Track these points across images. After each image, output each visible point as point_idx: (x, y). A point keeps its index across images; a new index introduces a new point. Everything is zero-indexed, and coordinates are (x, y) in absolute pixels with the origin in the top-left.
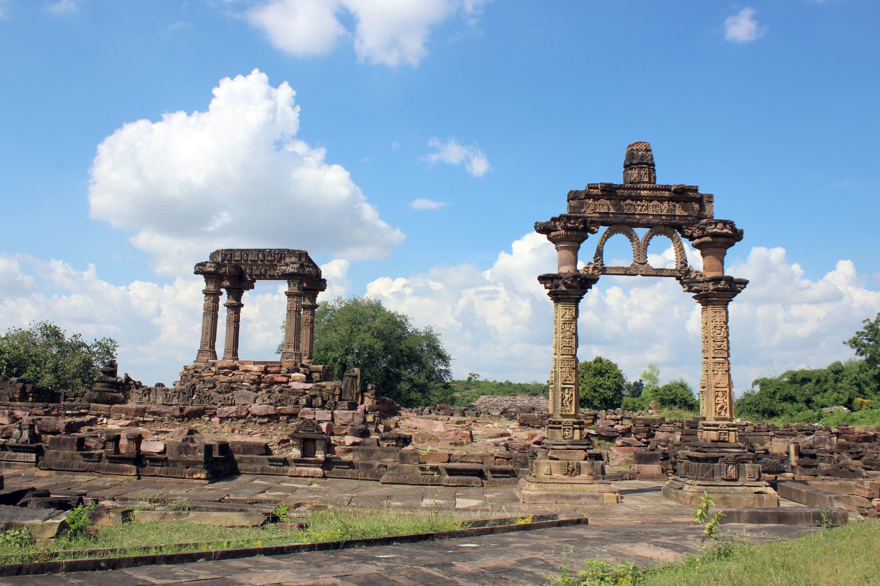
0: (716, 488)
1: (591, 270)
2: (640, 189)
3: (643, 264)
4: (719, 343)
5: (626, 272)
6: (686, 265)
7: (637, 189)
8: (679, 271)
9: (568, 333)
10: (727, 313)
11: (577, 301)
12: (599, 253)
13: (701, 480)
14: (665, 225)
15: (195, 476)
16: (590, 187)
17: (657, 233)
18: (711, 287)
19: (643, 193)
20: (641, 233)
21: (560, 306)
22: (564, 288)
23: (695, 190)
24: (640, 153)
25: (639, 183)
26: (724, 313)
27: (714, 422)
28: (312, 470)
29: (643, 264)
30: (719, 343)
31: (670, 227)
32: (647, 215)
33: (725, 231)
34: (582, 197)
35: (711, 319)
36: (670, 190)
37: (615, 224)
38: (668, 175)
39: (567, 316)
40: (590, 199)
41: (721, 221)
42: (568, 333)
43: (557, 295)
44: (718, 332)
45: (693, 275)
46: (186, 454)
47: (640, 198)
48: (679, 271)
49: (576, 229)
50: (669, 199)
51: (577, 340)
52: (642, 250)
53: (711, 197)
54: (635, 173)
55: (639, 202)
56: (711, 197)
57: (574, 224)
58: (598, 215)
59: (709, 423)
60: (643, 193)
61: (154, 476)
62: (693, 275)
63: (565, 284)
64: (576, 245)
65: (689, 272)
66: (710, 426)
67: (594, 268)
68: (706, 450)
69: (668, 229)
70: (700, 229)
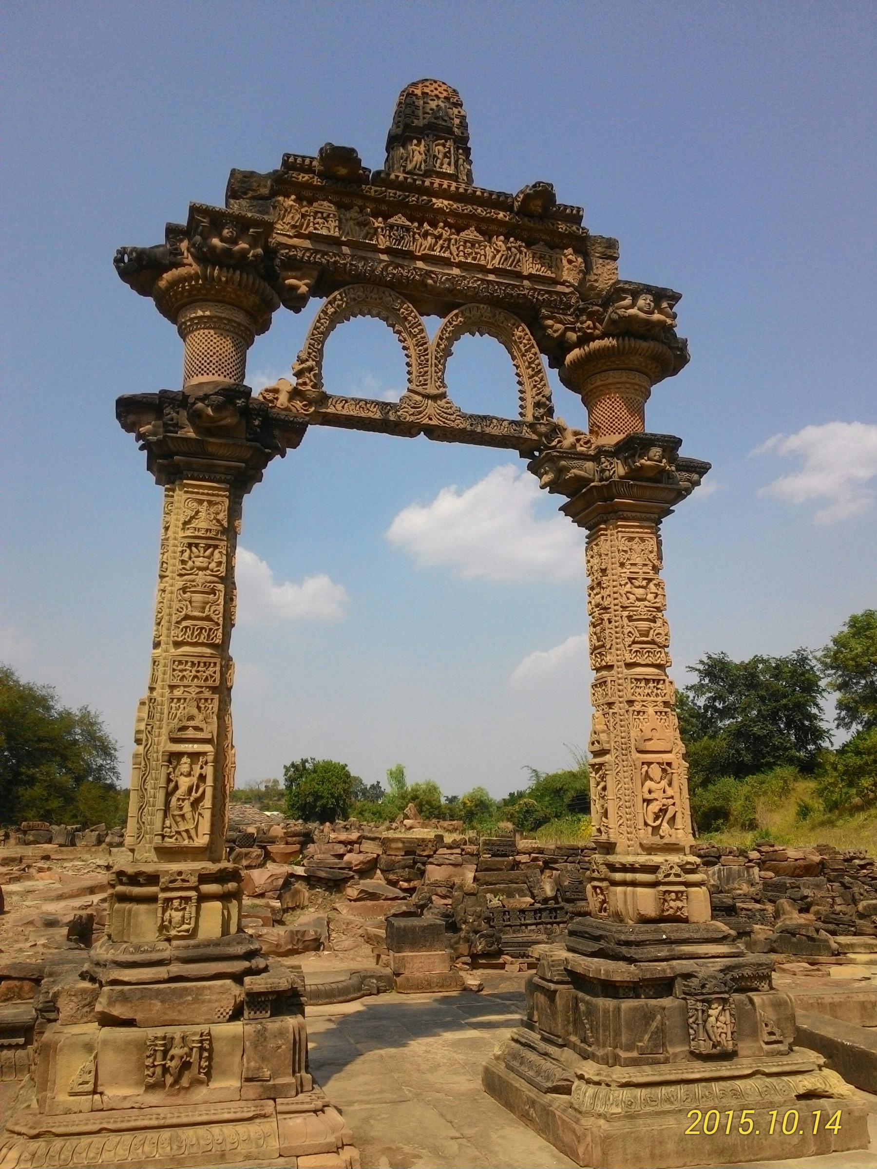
1: (283, 399)
3: (435, 398)
4: (644, 625)
5: (387, 422)
6: (550, 412)
8: (531, 426)
9: (201, 577)
10: (659, 543)
11: (241, 480)
13: (634, 1063)
14: (495, 302)
16: (291, 164)
17: (474, 326)
18: (621, 470)
19: (439, 203)
21: (180, 495)
22: (190, 433)
23: (575, 216)
24: (433, 104)
25: (429, 173)
26: (652, 544)
27: (643, 859)
29: (435, 398)
30: (644, 625)
31: (507, 311)
32: (447, 263)
33: (656, 316)
34: (265, 191)
35: (619, 557)
36: (509, 208)
37: (360, 279)
39: (202, 524)
40: (287, 196)
41: (648, 289)
42: (201, 577)
43: (170, 455)
44: (640, 592)
45: (570, 440)
47: (433, 217)
48: (531, 426)
49: (239, 262)
50: (509, 231)
51: (229, 599)
52: (430, 363)
53: (611, 244)
54: (417, 153)
55: (426, 226)
56: (611, 244)
57: (234, 241)
58: (307, 244)
59: (629, 859)
60: (439, 203)
62: (570, 440)
63: (196, 417)
64: (240, 318)
65: (557, 430)
66: (632, 869)
67: (295, 393)
68: (632, 952)
69: (501, 315)
70: (591, 316)
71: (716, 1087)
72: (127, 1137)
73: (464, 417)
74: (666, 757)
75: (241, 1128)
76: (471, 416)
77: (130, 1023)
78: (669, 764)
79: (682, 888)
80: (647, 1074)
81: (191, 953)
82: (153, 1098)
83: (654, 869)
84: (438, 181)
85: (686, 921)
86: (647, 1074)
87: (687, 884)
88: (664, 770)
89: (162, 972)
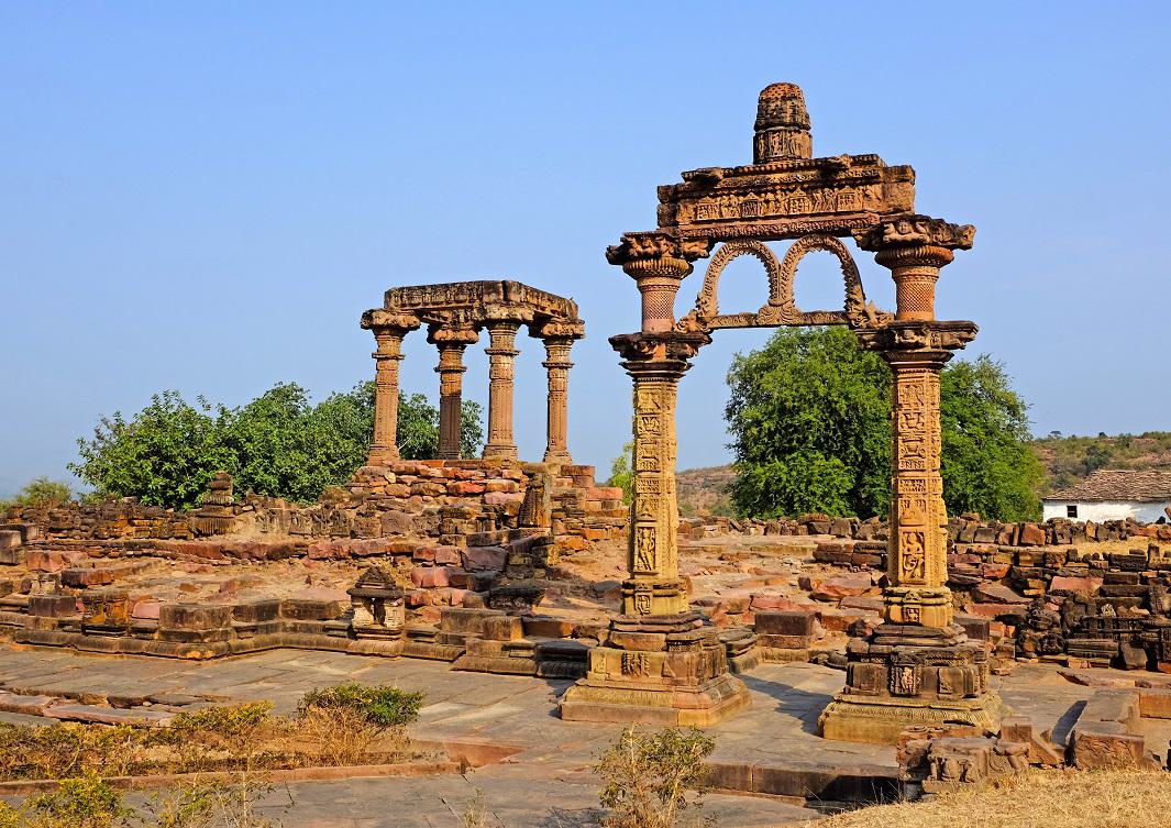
0: (878, 708)
2: (771, 172)
7: (766, 172)
12: (708, 288)
15: (189, 656)
20: (779, 249)
28: (379, 644)
38: (824, 144)
46: (182, 623)
56: (903, 170)
60: (776, 178)
61: (142, 653)
71: (898, 710)
72: (615, 691)
73: (799, 315)
74: (919, 529)
75: (659, 695)
76: (805, 314)
77: (622, 648)
78: (922, 534)
79: (919, 606)
80: (864, 699)
81: (648, 620)
82: (626, 678)
83: (903, 595)
84: (774, 163)
85: (921, 625)
86: (864, 699)
87: (922, 604)
88: (918, 537)
89: (635, 628)
